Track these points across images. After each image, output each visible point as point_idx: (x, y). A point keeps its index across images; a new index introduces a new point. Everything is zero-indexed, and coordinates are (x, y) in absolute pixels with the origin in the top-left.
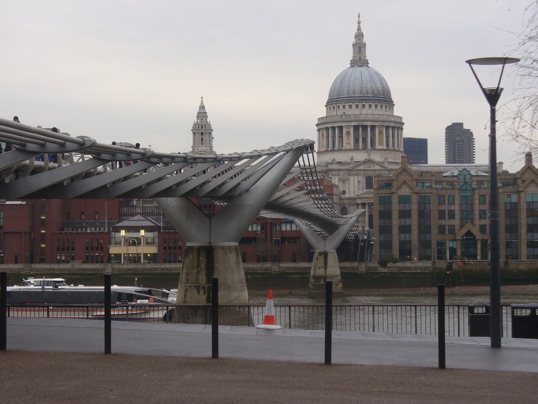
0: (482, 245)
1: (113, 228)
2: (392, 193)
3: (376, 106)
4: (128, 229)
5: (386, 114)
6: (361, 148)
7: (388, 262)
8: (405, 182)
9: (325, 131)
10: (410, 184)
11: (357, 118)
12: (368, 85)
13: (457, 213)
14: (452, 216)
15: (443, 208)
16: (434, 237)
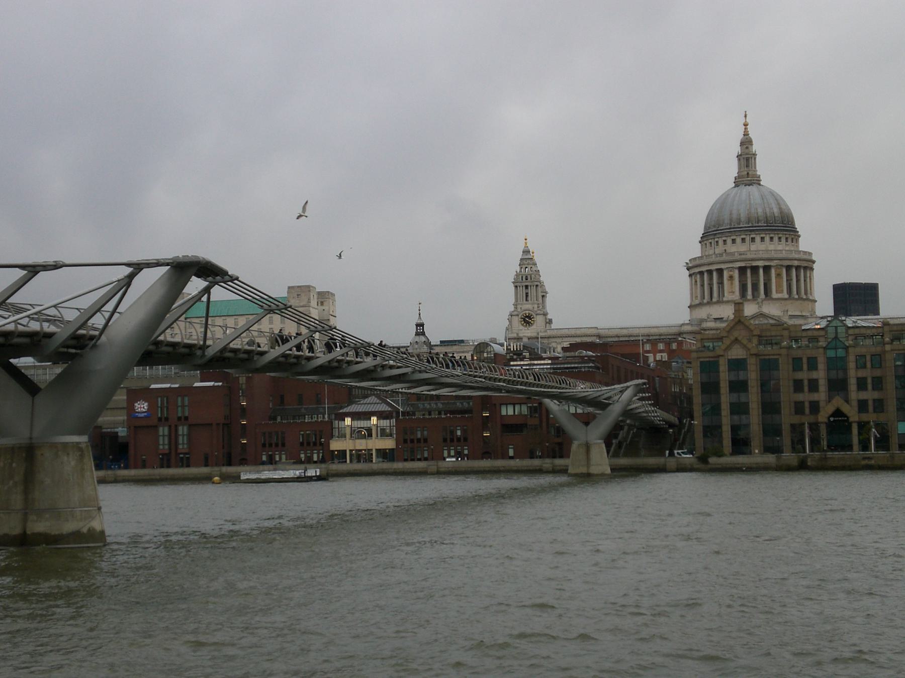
0: (811, 429)
1: (336, 414)
2: (719, 356)
3: (771, 239)
4: (356, 416)
5: (787, 248)
6: (749, 296)
8: (736, 339)
9: (698, 276)
10: (745, 342)
11: (743, 256)
12: (760, 211)
14: (814, 386)
15: (800, 375)
16: (787, 418)
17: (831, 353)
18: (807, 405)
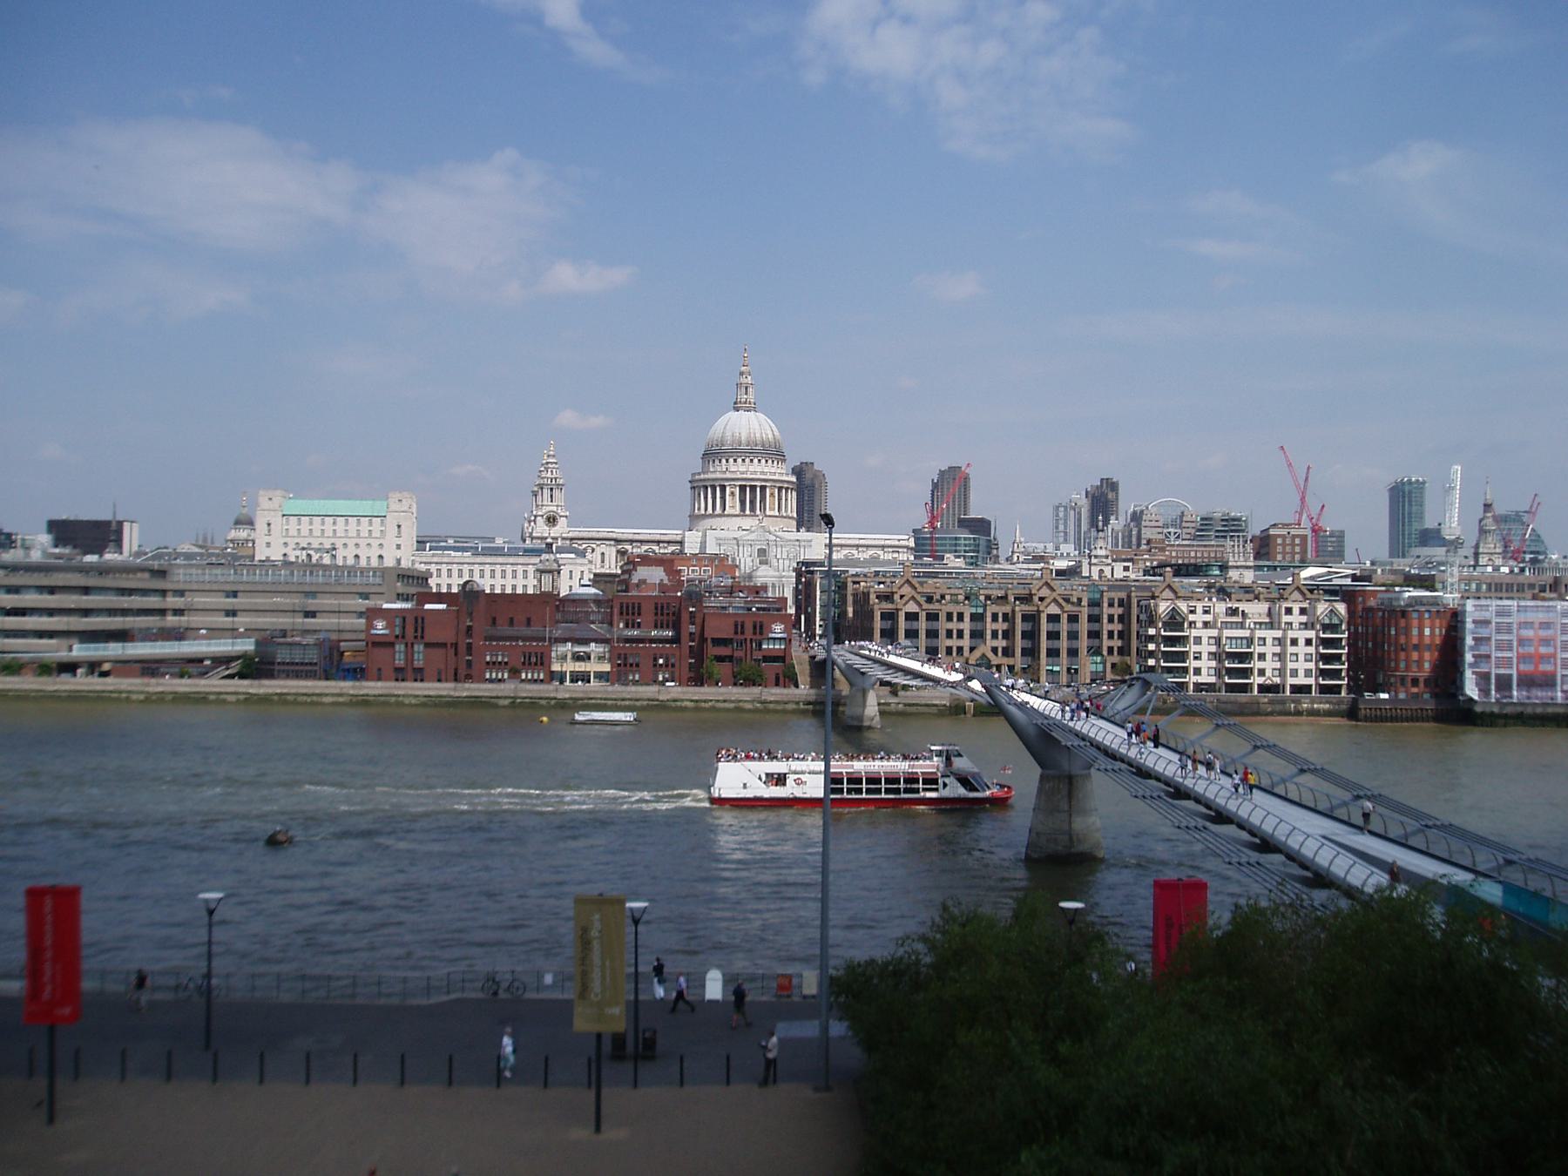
14: (960, 634)
15: (950, 626)
17: (973, 610)
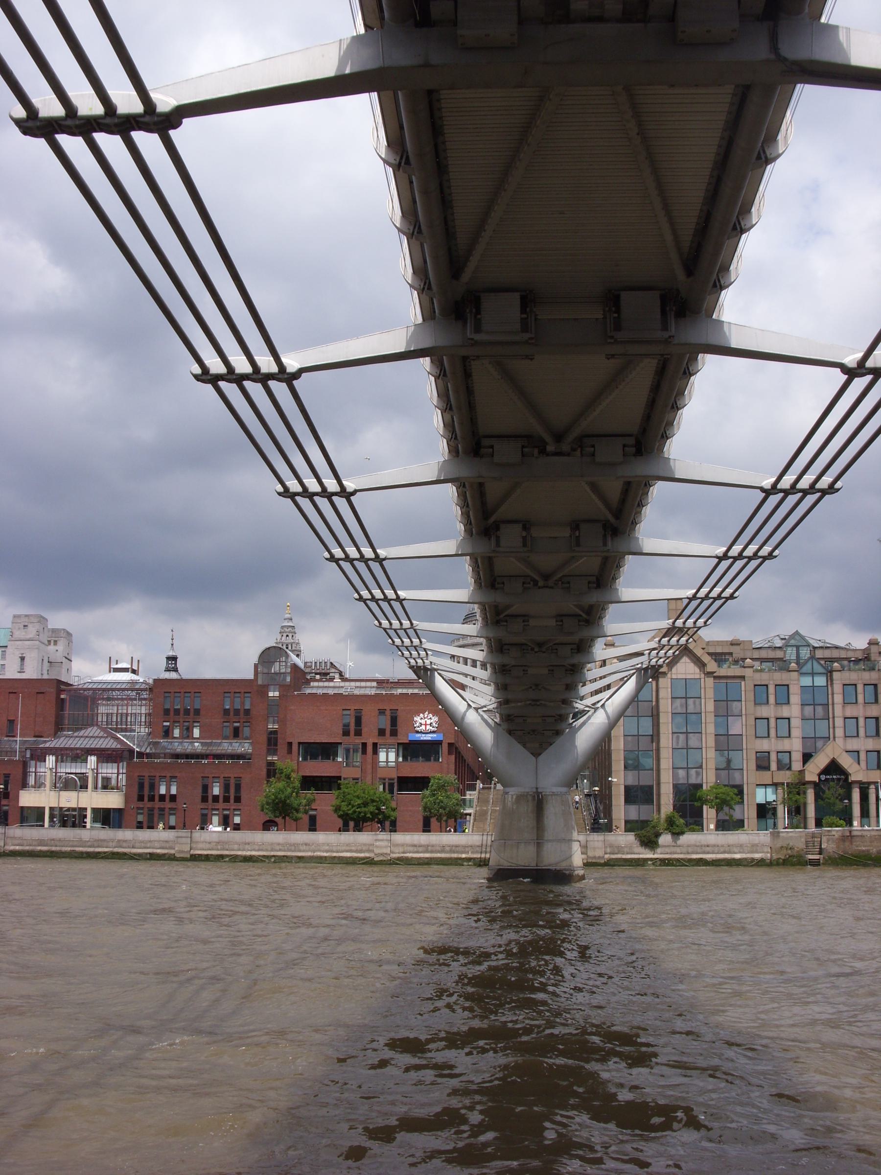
4: (62, 755)
7: (658, 835)
13: (796, 722)
17: (807, 681)
18: (773, 757)
